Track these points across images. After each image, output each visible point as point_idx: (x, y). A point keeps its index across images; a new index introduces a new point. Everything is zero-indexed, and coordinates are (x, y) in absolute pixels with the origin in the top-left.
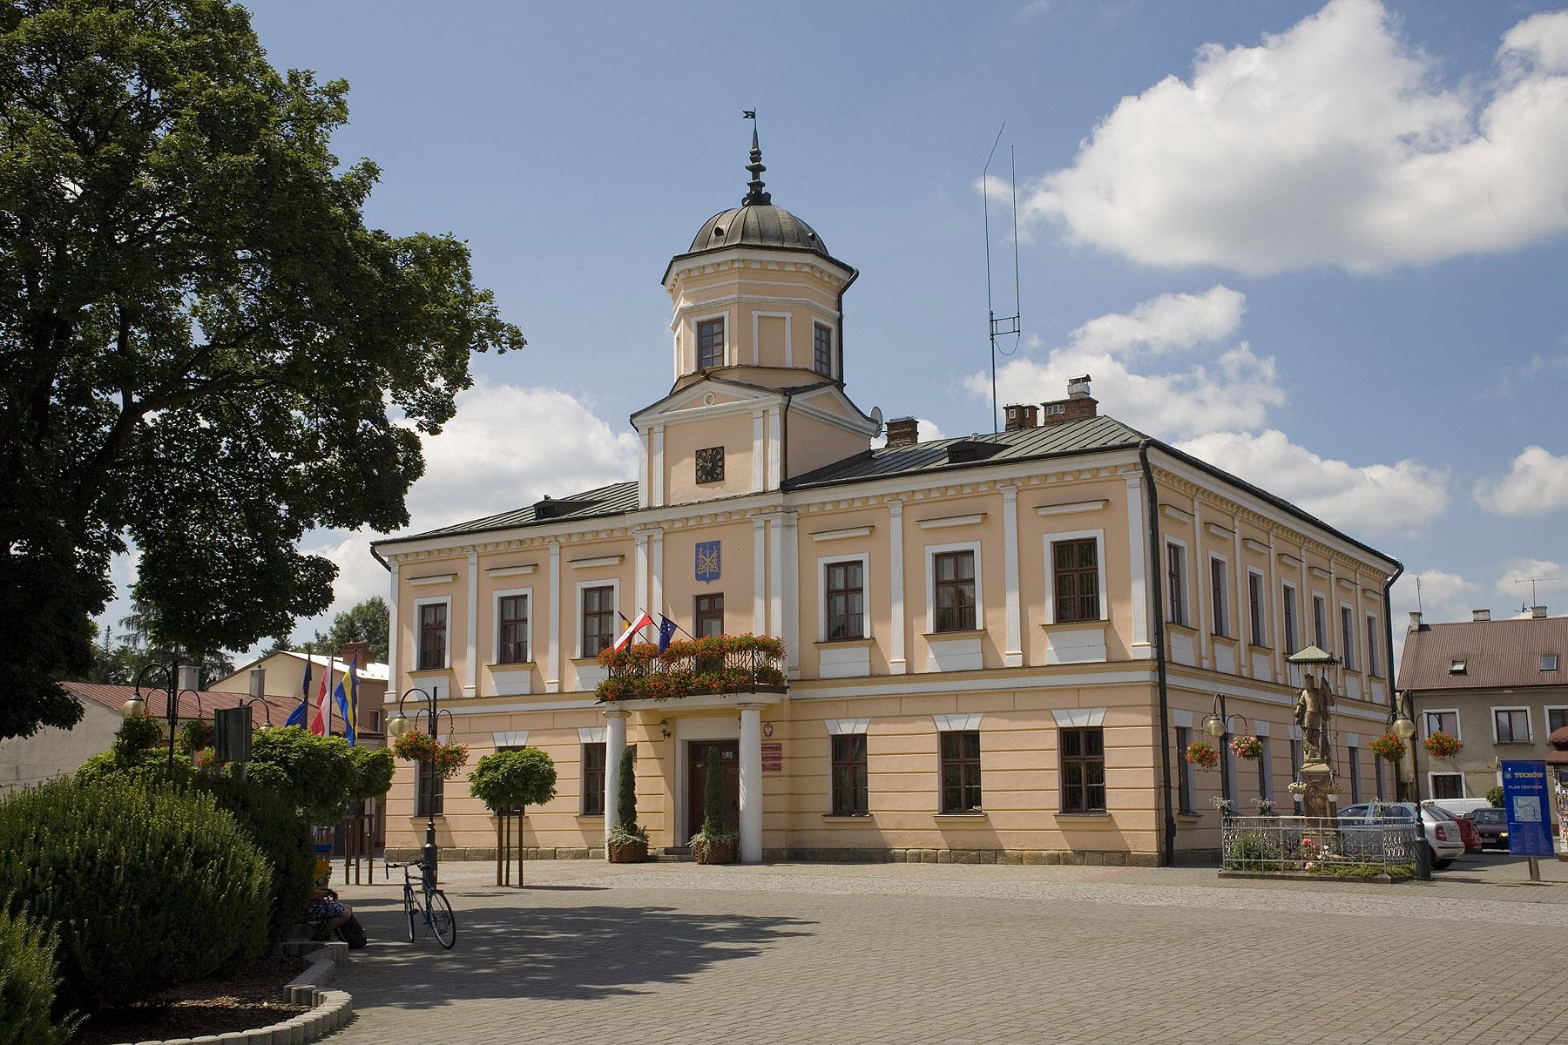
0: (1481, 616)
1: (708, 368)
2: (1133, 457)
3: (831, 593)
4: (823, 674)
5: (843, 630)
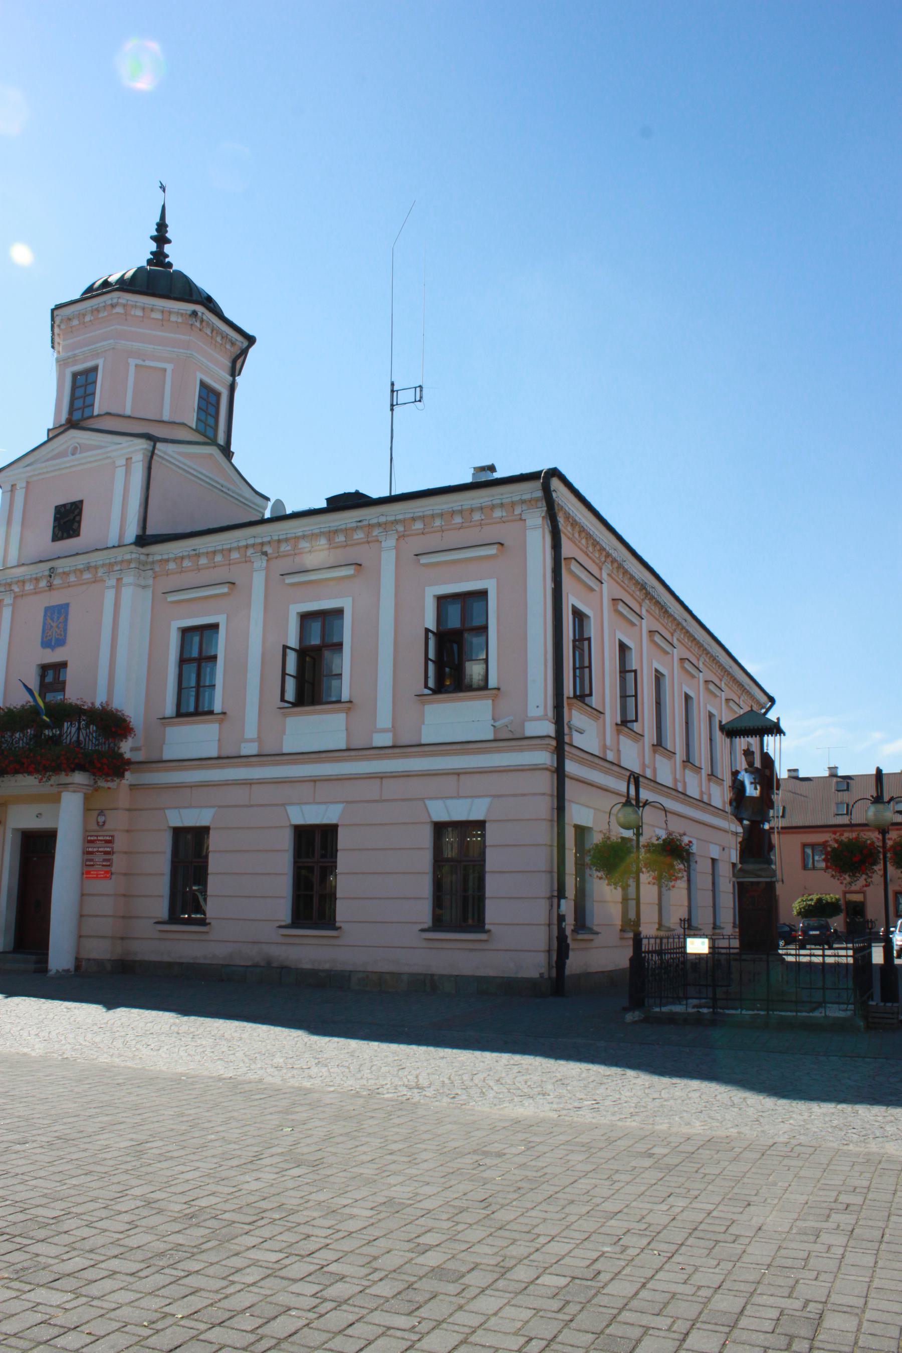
0: (794, 774)
1: (77, 416)
2: (534, 490)
3: (183, 661)
4: (166, 757)
5: (193, 704)
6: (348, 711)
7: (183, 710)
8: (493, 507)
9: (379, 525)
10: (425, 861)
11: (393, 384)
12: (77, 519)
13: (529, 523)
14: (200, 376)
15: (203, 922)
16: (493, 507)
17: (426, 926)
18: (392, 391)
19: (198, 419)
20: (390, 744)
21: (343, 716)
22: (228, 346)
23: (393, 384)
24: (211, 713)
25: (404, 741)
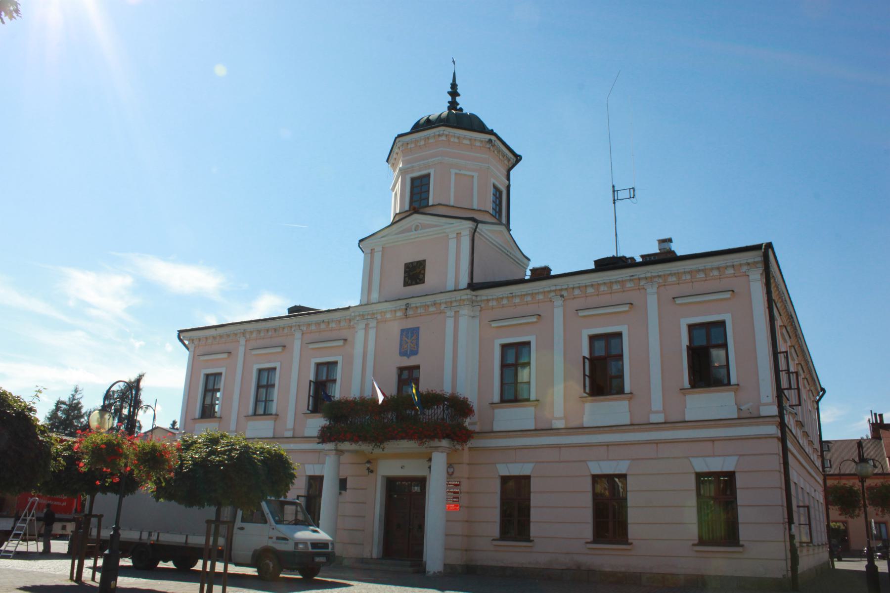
1: (416, 205)
2: (757, 256)
4: (496, 429)
5: (512, 394)
6: (630, 399)
7: (506, 398)
8: (726, 267)
9: (646, 278)
11: (613, 187)
13: (751, 277)
14: (493, 180)
15: (528, 539)
16: (726, 267)
18: (614, 191)
20: (663, 421)
21: (626, 403)
22: (506, 162)
23: (613, 187)
24: (528, 400)
25: (669, 420)
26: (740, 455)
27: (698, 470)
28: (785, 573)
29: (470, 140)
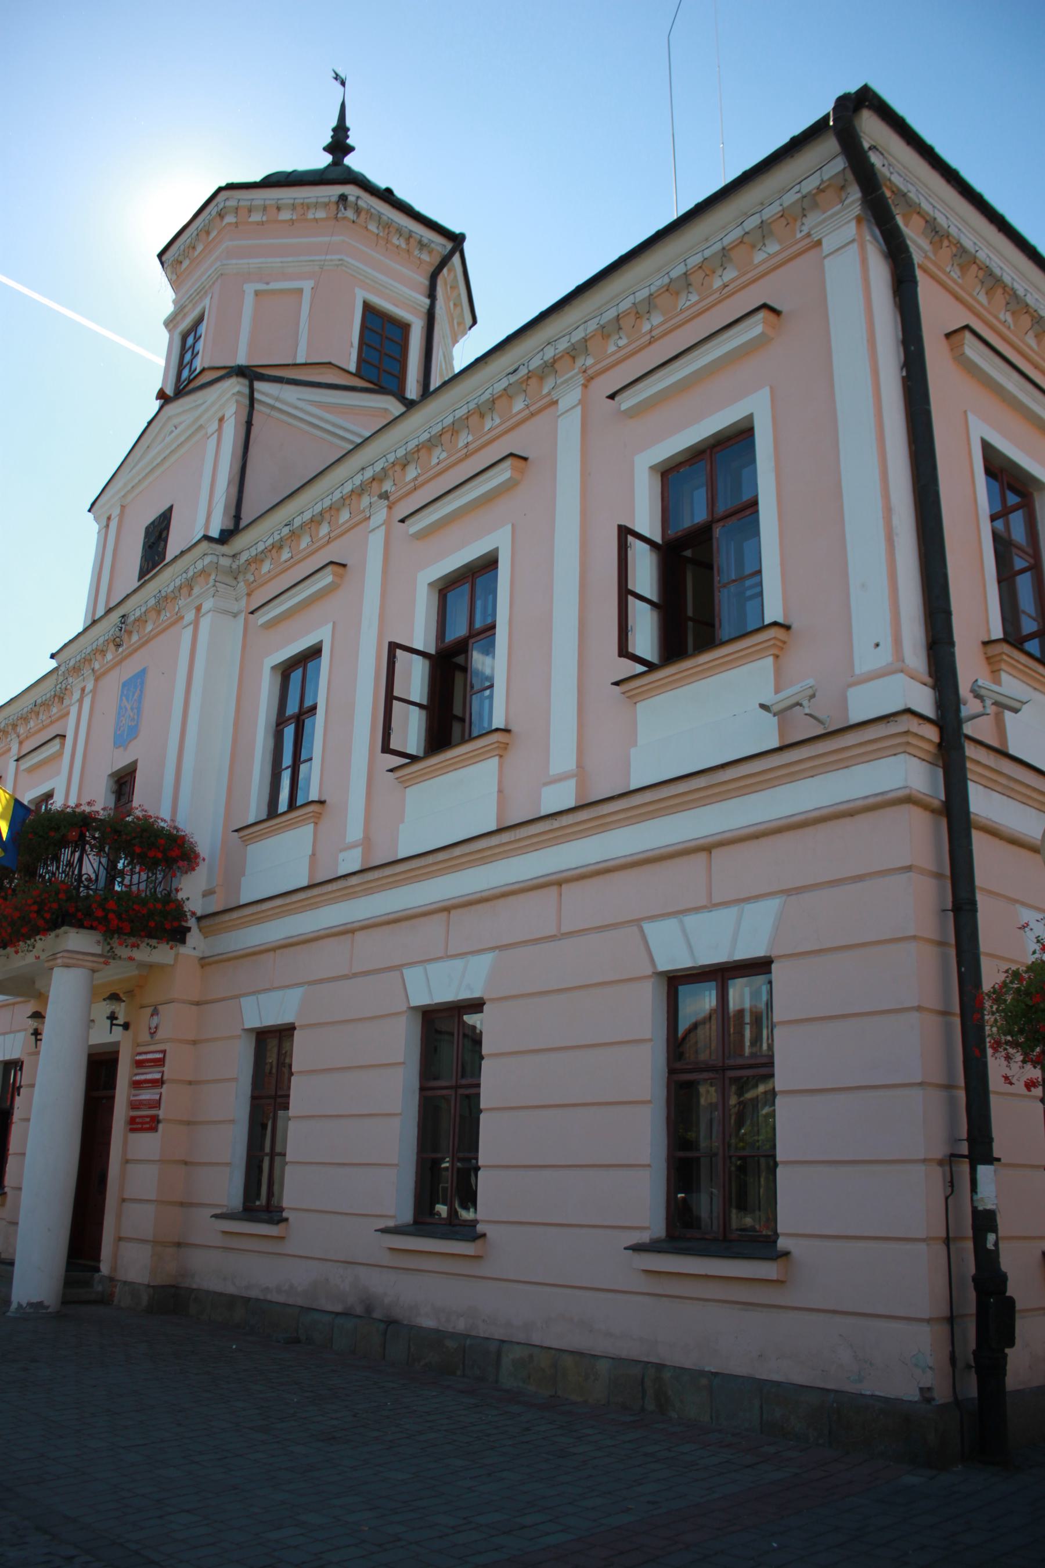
5: (286, 797)
10: (644, 1074)
12: (164, 535)
17: (645, 1237)
19: (361, 360)
26: (788, 892)
27: (664, 966)
28: (927, 1380)
29: (294, 207)
